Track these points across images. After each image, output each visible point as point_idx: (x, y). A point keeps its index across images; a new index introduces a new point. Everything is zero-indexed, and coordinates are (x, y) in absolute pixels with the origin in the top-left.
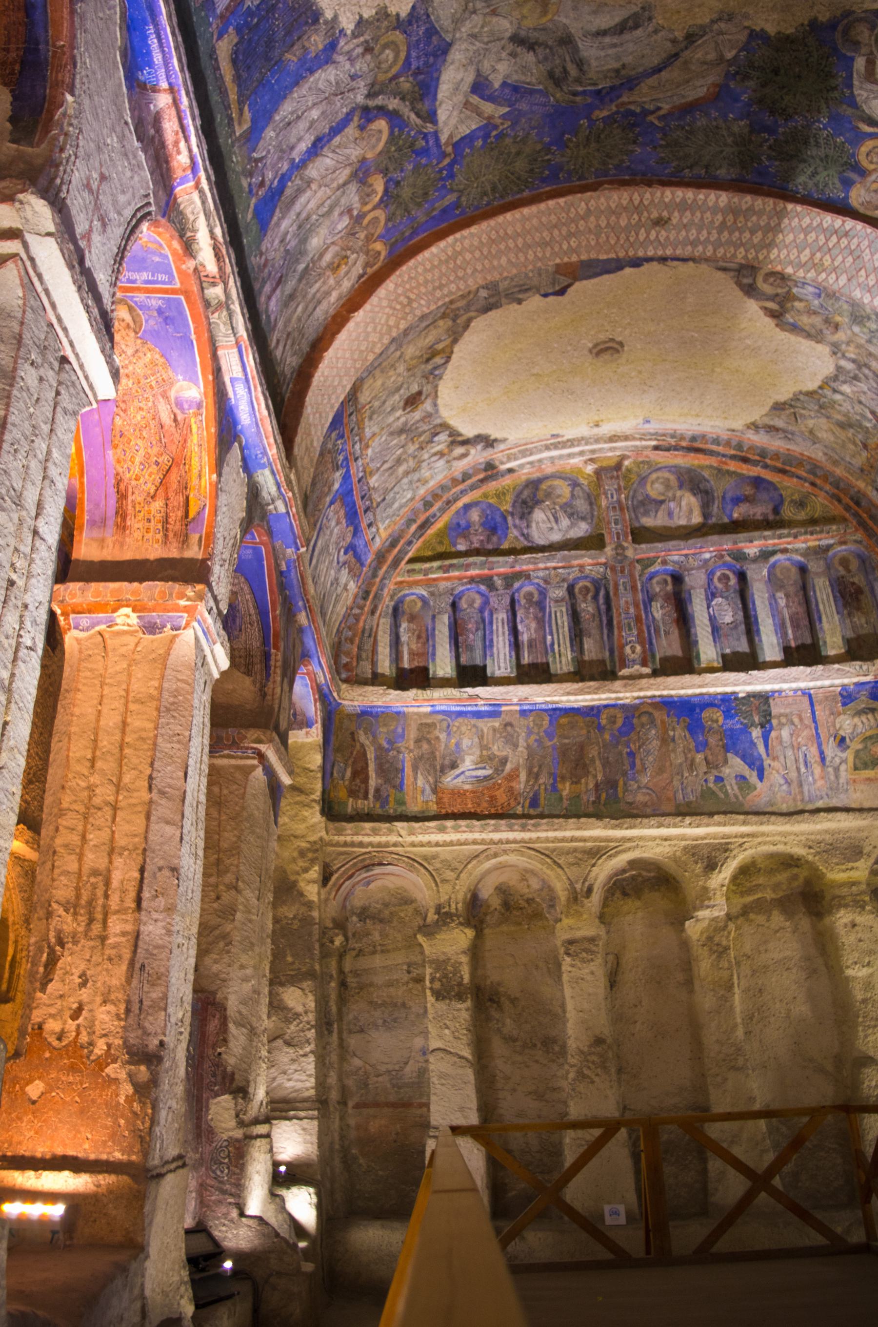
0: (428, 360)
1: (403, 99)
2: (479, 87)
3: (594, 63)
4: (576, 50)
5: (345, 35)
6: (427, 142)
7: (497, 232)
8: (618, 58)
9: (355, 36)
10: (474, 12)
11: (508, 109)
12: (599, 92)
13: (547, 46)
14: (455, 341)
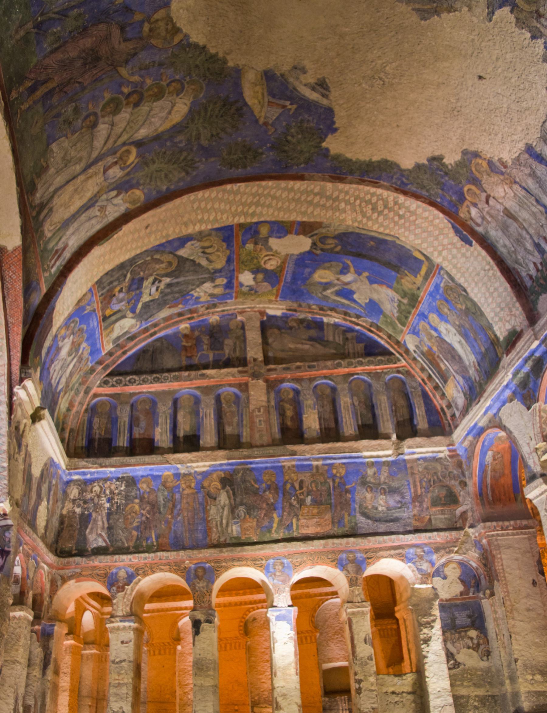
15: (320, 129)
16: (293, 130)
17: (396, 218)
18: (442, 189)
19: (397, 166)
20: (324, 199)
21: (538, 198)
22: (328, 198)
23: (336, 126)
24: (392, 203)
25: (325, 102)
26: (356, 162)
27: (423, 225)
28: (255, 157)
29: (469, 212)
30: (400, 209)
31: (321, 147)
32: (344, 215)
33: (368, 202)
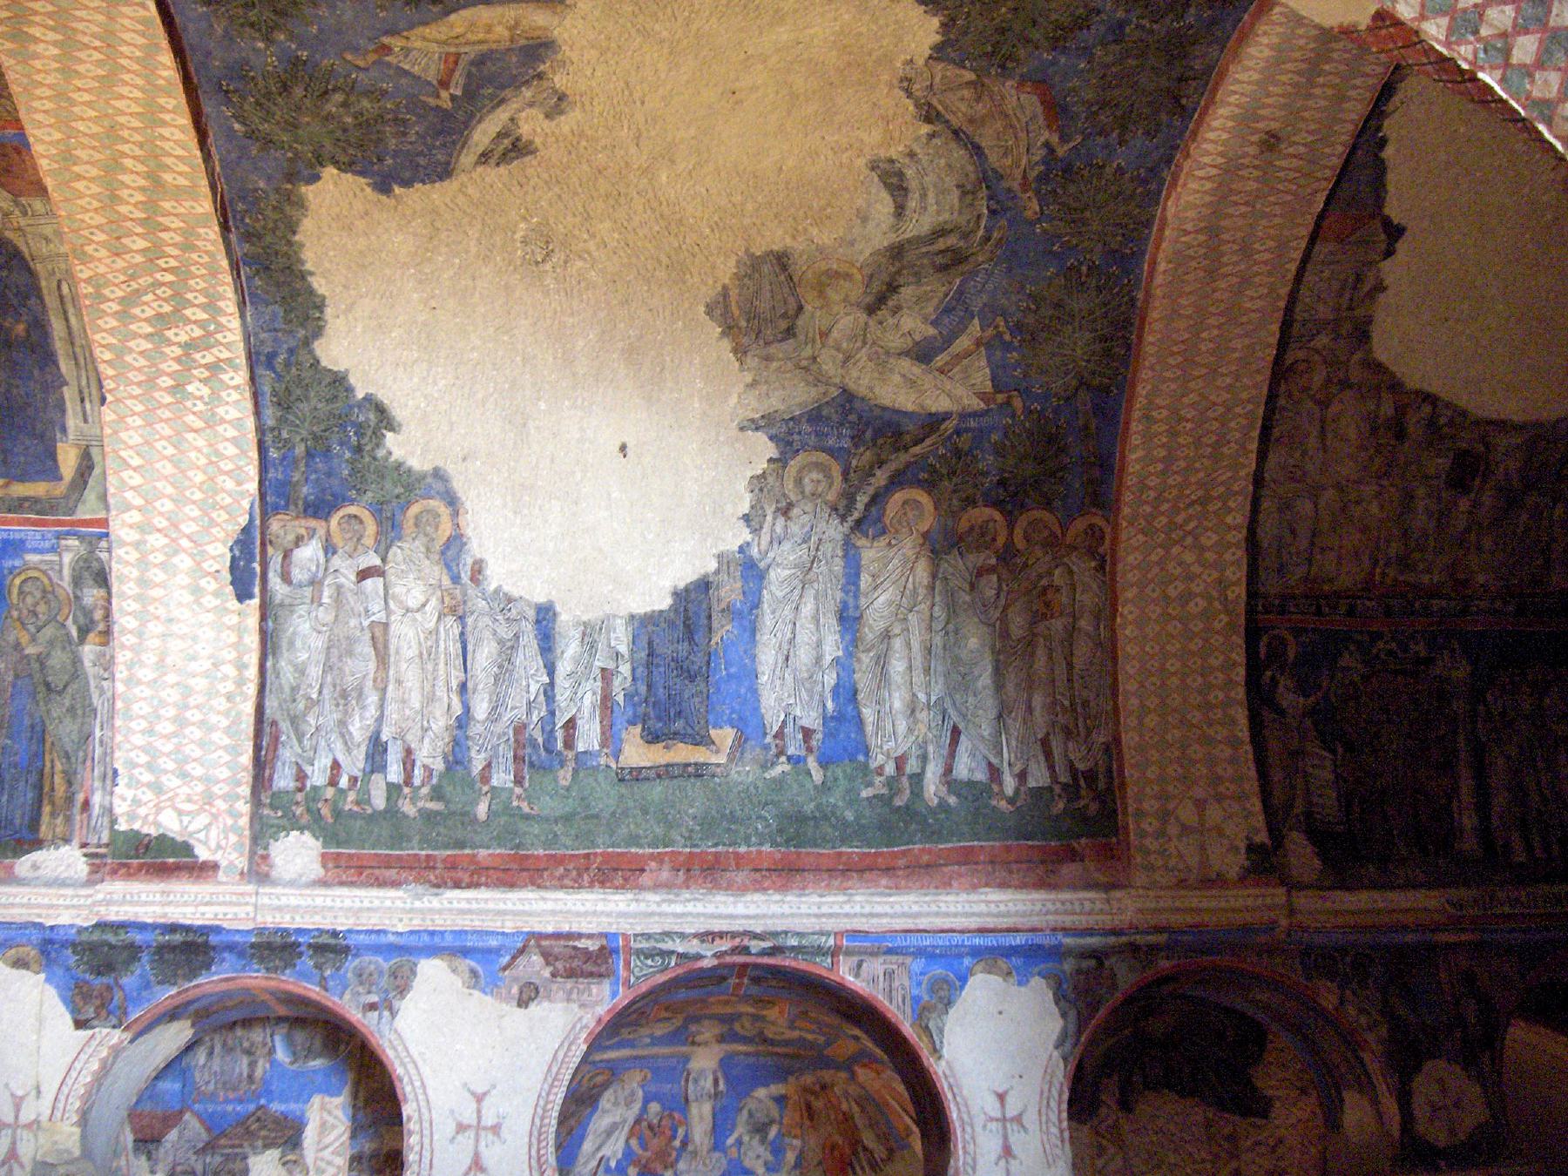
0: (1401, 435)
1: (881, 464)
2: (923, 353)
3: (947, 216)
4: (917, 241)
5: (748, 544)
6: (967, 430)
7: (1172, 354)
8: (944, 192)
9: (756, 531)
10: (814, 359)
11: (976, 321)
12: (993, 212)
13: (899, 272)
14: (1395, 386)
15: (380, 160)
16: (366, 103)
17: (166, 382)
18: (309, 454)
19: (318, 332)
20: (139, 197)
21: (470, 685)
22: (150, 205)
23: (397, 190)
24: (209, 359)
25: (467, 159)
26: (290, 243)
27: (193, 455)
28: (252, 25)
29: (298, 541)
30: (205, 381)
31: (323, 166)
32: (103, 253)
33: (179, 300)
